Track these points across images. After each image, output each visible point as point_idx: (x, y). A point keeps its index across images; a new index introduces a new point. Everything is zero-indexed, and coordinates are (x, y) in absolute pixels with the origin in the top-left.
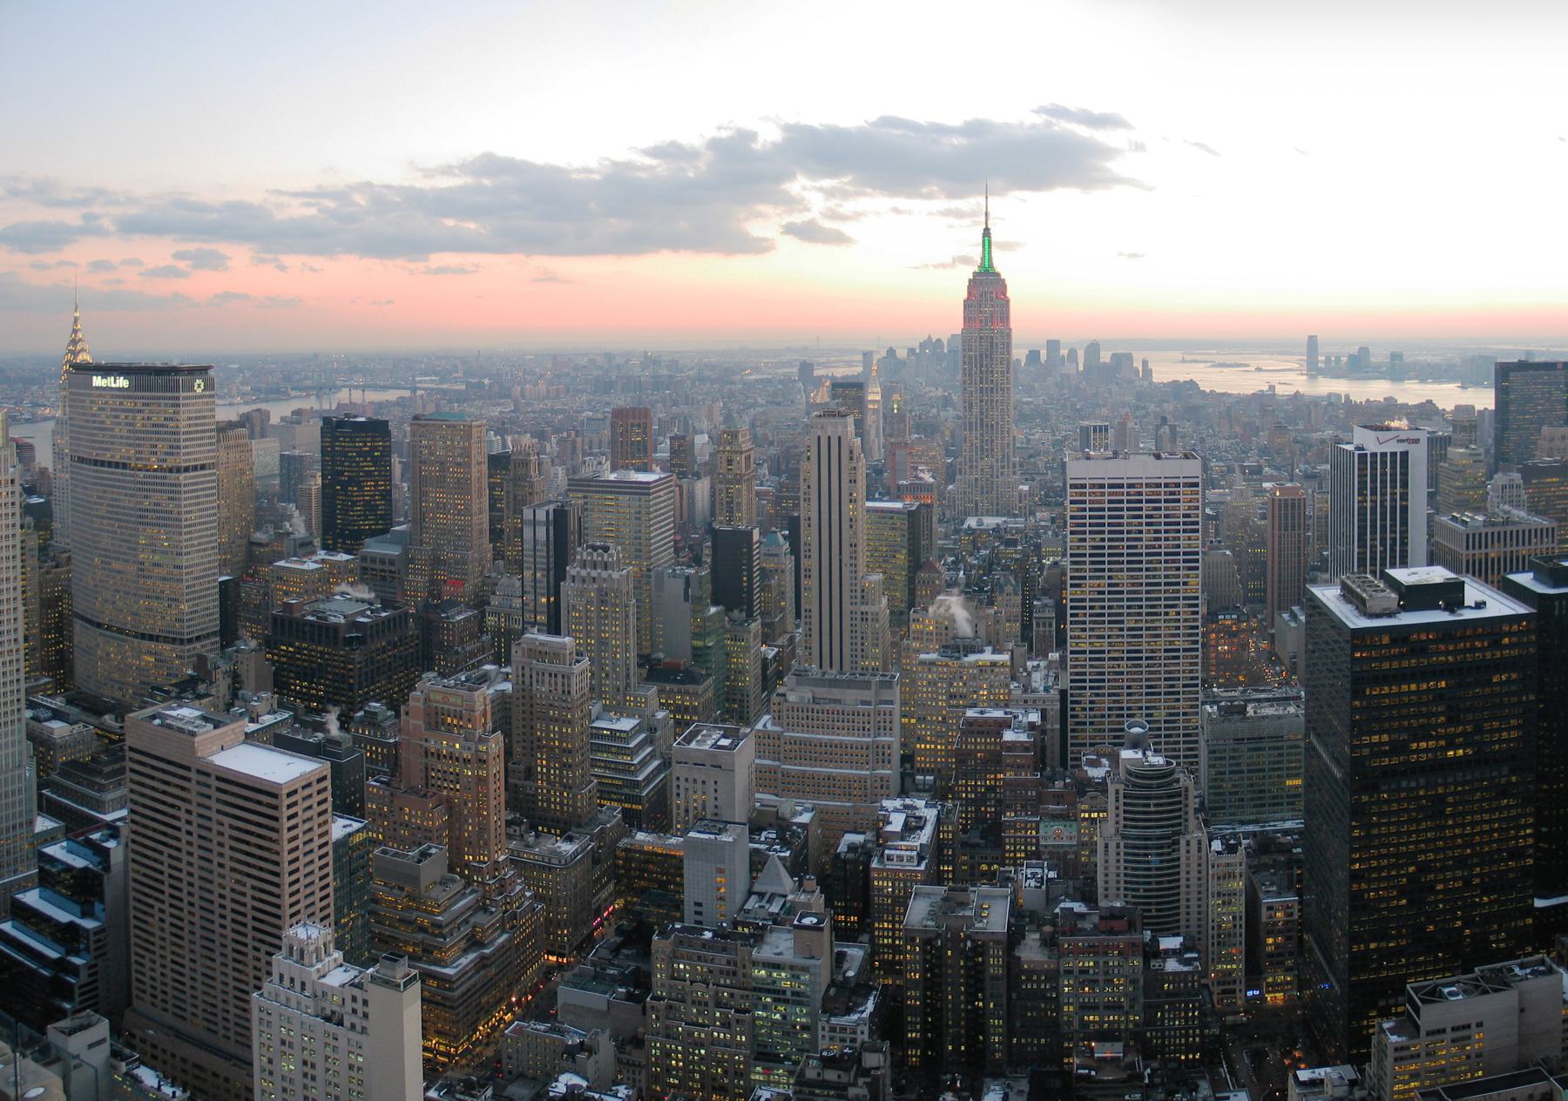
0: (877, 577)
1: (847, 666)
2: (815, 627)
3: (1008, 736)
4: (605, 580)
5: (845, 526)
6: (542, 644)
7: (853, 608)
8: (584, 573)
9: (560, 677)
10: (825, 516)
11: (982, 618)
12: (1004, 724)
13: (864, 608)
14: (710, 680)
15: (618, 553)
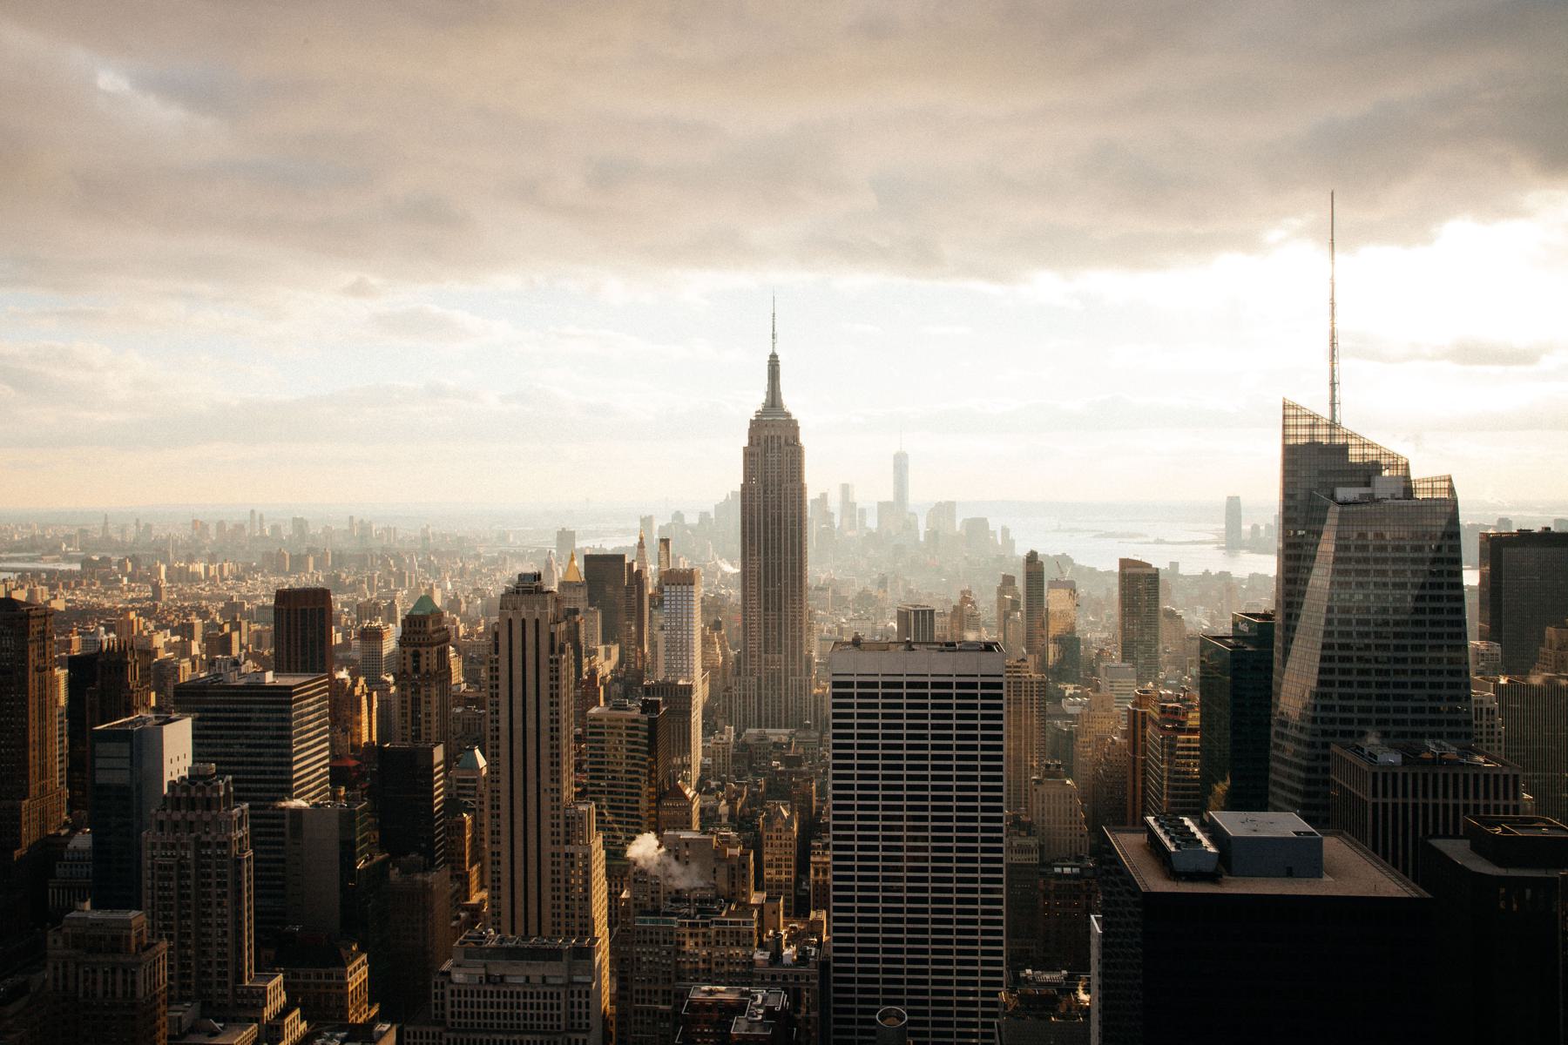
0: (588, 808)
1: (547, 928)
2: (505, 877)
3: (739, 1027)
4: (207, 824)
5: (545, 738)
6: (96, 924)
7: (555, 849)
8: (177, 816)
9: (119, 976)
10: (518, 726)
11: (724, 860)
12: (739, 1008)
13: (569, 849)
14: (364, 957)
15: (227, 785)
